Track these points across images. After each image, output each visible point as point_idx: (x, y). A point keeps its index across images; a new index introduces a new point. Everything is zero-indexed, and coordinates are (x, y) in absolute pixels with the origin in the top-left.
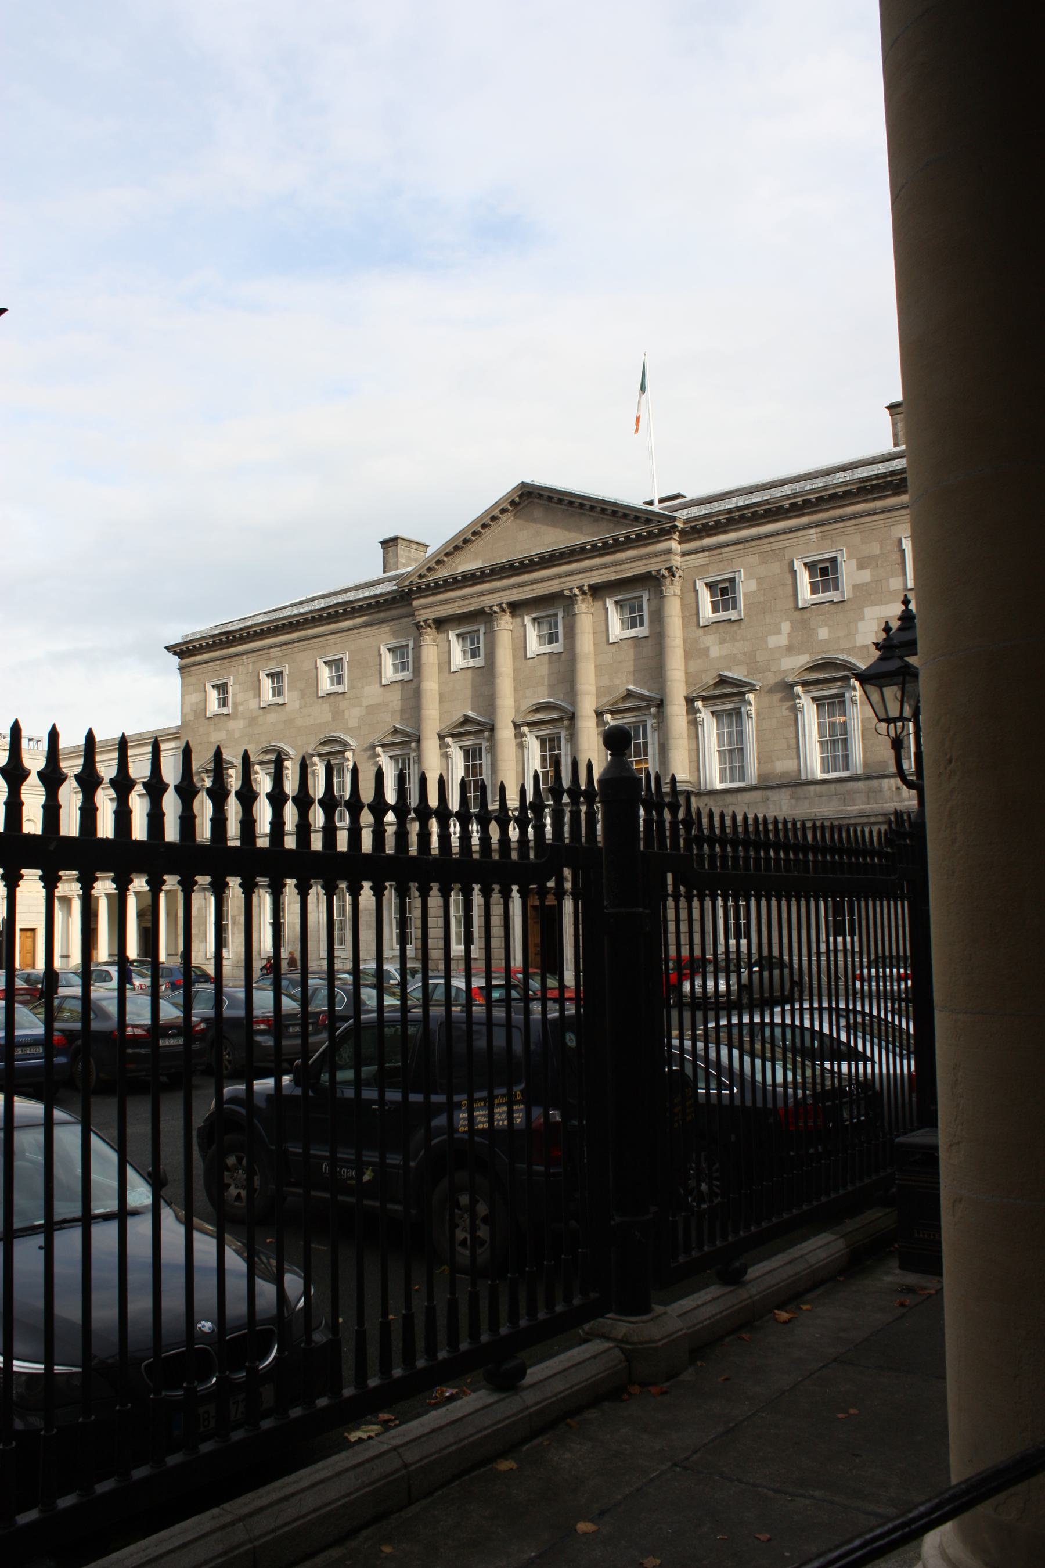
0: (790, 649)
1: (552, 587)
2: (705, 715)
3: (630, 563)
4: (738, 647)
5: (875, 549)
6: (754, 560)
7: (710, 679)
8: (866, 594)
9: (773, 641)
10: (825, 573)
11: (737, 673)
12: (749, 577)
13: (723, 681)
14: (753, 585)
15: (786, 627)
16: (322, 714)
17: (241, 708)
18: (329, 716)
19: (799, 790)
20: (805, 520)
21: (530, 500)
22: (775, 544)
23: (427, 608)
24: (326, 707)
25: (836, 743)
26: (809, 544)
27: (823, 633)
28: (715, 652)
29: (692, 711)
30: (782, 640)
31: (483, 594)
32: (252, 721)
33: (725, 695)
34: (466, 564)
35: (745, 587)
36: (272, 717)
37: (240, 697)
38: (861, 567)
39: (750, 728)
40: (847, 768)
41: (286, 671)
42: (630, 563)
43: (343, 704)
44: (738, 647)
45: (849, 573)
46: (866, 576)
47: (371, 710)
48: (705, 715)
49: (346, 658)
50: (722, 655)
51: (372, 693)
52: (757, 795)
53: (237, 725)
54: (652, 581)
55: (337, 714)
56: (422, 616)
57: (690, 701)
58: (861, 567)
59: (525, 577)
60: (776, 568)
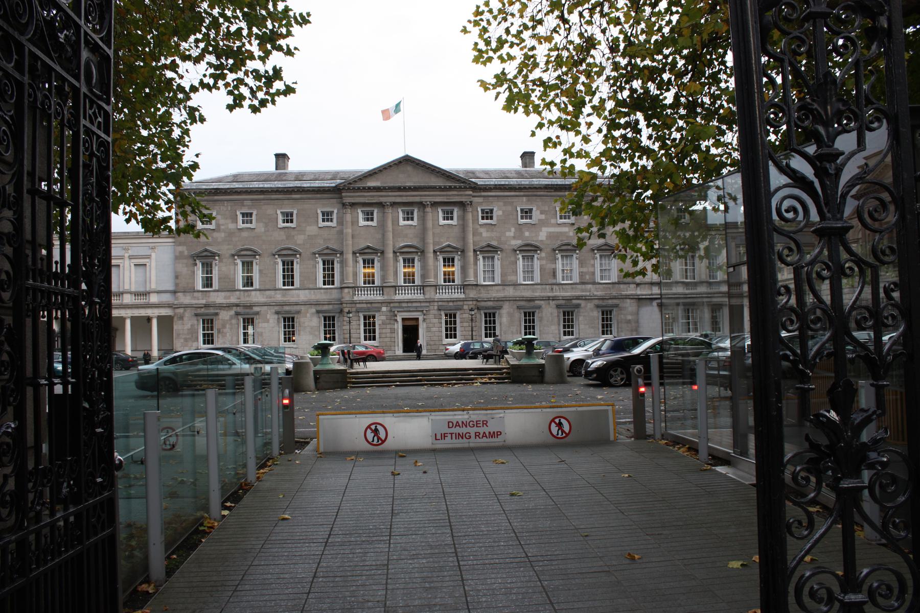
0: (514, 238)
1: (417, 199)
2: (480, 257)
3: (454, 196)
4: (494, 234)
5: (547, 209)
6: (501, 204)
7: (484, 244)
8: (542, 223)
9: (508, 234)
10: (527, 213)
11: (494, 243)
12: (499, 209)
13: (489, 246)
14: (500, 213)
15: (513, 230)
16: (281, 236)
17: (222, 227)
18: (284, 237)
19: (518, 287)
20: (522, 194)
21: (407, 161)
22: (510, 200)
23: (349, 198)
24: (282, 233)
25: (529, 272)
26: (522, 203)
27: (527, 234)
28: (485, 234)
29: (476, 256)
30: (512, 234)
31: (382, 196)
32: (231, 234)
33: (489, 251)
34: (372, 183)
35: (497, 213)
36: (245, 234)
37: (222, 221)
38: (541, 213)
39: (497, 263)
40: (532, 280)
41: (255, 213)
42: (454, 196)
43: (293, 233)
44: (494, 234)
45: (536, 214)
46: (543, 217)
47: (311, 237)
48: (480, 257)
49: (295, 212)
50: (486, 236)
51: (312, 230)
52: (501, 287)
53: (220, 236)
54: (462, 205)
55: (289, 237)
56: (347, 200)
57: (475, 251)
58: (541, 213)
59: (404, 193)
60: (509, 208)
